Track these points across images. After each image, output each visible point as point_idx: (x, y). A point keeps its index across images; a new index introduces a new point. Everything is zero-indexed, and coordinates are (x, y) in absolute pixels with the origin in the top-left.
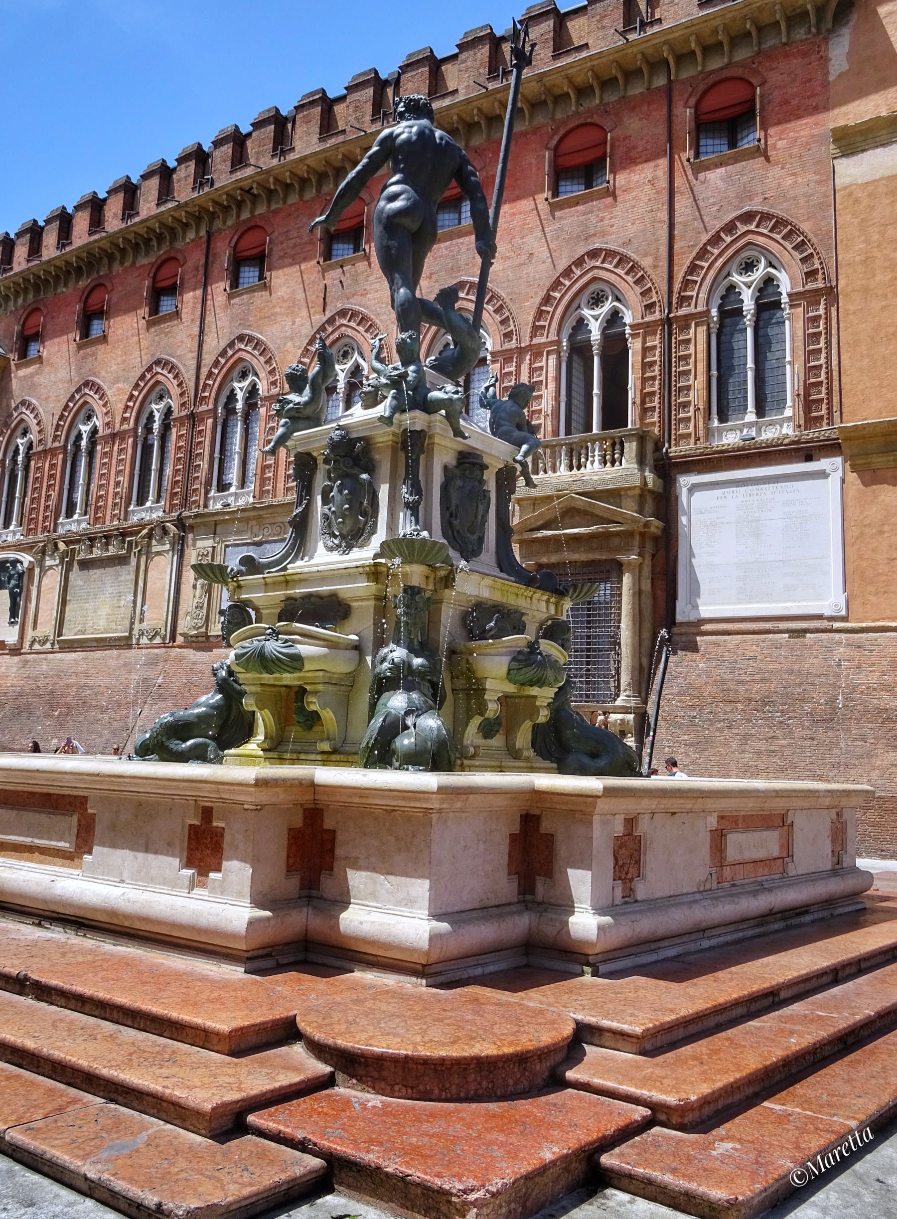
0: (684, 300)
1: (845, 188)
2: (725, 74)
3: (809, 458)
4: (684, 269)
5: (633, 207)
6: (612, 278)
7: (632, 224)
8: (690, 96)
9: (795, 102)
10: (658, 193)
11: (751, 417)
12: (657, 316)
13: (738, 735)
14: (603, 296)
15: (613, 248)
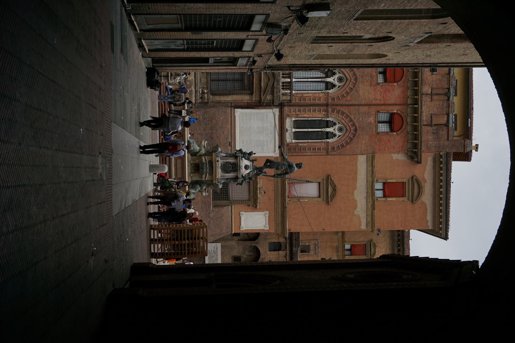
0: (333, 111)
1: (357, 158)
2: (405, 123)
3: (279, 147)
4: (343, 110)
5: (369, 93)
6: (346, 86)
7: (363, 92)
8: (401, 111)
9: (388, 144)
10: (371, 101)
11: (294, 130)
12: (330, 101)
13: (202, 132)
14: (341, 81)
15: (356, 85)
